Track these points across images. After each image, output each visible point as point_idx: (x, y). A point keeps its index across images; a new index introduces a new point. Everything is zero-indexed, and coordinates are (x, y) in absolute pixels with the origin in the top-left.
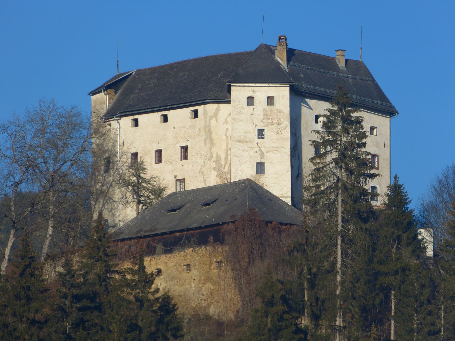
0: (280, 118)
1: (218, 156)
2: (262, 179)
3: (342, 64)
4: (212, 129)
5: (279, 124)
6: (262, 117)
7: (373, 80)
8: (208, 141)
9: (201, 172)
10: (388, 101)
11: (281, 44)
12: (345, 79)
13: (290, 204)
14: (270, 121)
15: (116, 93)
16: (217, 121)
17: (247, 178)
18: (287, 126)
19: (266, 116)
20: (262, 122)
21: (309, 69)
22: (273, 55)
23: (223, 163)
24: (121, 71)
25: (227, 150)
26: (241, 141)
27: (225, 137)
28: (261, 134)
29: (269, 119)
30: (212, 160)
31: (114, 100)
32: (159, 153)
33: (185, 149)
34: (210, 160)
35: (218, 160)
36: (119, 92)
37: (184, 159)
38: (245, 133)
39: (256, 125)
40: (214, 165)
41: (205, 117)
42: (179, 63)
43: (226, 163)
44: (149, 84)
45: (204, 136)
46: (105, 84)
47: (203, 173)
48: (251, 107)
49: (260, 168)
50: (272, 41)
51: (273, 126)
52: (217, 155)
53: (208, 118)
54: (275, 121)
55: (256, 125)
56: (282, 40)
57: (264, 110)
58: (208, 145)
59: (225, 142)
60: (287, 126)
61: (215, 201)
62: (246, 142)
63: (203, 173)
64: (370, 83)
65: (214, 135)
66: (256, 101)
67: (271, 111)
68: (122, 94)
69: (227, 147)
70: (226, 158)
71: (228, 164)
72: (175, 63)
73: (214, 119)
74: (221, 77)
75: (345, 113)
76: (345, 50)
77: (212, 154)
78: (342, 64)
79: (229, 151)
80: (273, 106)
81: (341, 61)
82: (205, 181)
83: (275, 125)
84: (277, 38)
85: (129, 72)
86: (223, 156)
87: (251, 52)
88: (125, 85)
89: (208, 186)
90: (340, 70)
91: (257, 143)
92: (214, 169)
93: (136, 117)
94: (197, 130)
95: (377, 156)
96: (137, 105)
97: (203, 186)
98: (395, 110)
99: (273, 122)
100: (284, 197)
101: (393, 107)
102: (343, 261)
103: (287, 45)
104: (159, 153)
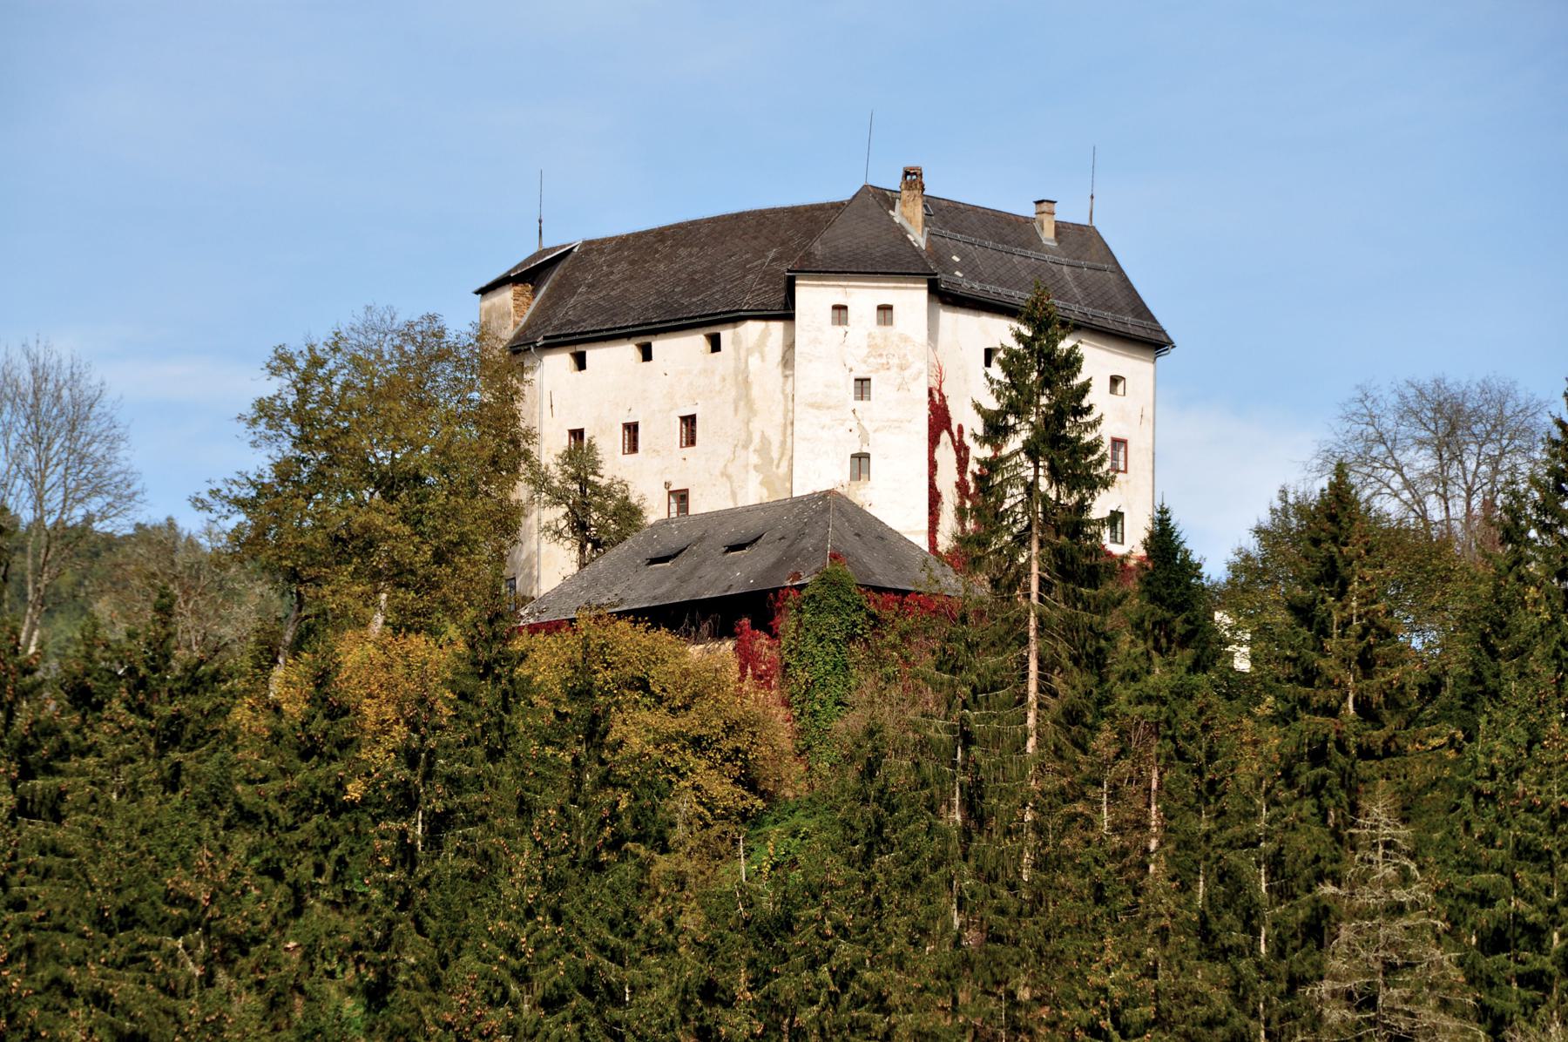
0: (905, 355)
1: (763, 437)
2: (862, 491)
3: (1048, 235)
4: (751, 377)
5: (902, 368)
6: (865, 351)
7: (1119, 271)
8: (742, 404)
9: (725, 474)
10: (1152, 318)
11: (909, 186)
12: (1055, 268)
13: (927, 549)
14: (884, 360)
15: (535, 292)
16: (763, 358)
17: (830, 488)
18: (920, 373)
19: (874, 349)
20: (865, 362)
21: (972, 244)
22: (891, 212)
23: (775, 454)
24: (547, 245)
25: (785, 424)
26: (812, 406)
27: (781, 396)
28: (863, 384)
29: (881, 355)
30: (751, 448)
31: (528, 312)
32: (632, 429)
33: (689, 421)
34: (746, 447)
35: (764, 450)
36: (544, 289)
37: (687, 445)
38: (826, 386)
39: (851, 370)
40: (754, 459)
41: (737, 350)
42: (680, 226)
43: (782, 454)
44: (612, 273)
45: (733, 393)
46: (510, 272)
47: (729, 477)
48: (841, 329)
49: (861, 461)
50: (892, 181)
51: (888, 373)
52: (763, 437)
53: (743, 353)
54: (894, 361)
55: (851, 370)
56: (912, 177)
57: (870, 335)
58: (742, 413)
59: (781, 407)
60: (920, 373)
61: (755, 541)
62: (829, 408)
63: (729, 477)
64: (1111, 276)
65: (755, 392)
66: (852, 314)
67: (886, 339)
68: (548, 296)
69: (785, 418)
70: (783, 443)
71: (786, 458)
72: (671, 227)
73: (757, 355)
74: (773, 260)
75: (1039, 745)
76: (1054, 202)
77: (749, 434)
78: (1048, 235)
79: (789, 428)
80: (888, 328)
81: (1046, 225)
82: (734, 495)
83: (894, 370)
84: (901, 173)
85: (564, 246)
86: (775, 439)
87: (842, 203)
88: (556, 274)
89: (740, 505)
90: (1043, 245)
91: (854, 411)
92: (755, 467)
93: (580, 348)
94: (717, 379)
95: (1124, 442)
96: (584, 321)
97: (729, 505)
98: (1168, 338)
99: (891, 362)
100: (911, 533)
101: (1163, 332)
102: (1040, 676)
103: (923, 190)
104: (632, 429)
